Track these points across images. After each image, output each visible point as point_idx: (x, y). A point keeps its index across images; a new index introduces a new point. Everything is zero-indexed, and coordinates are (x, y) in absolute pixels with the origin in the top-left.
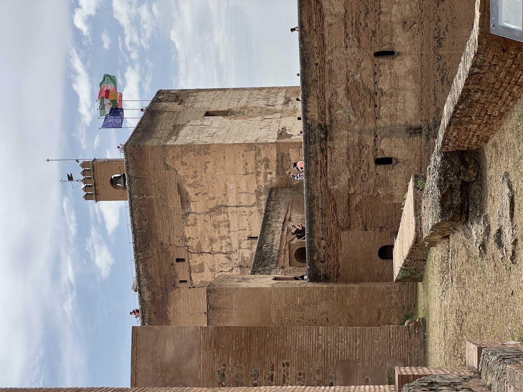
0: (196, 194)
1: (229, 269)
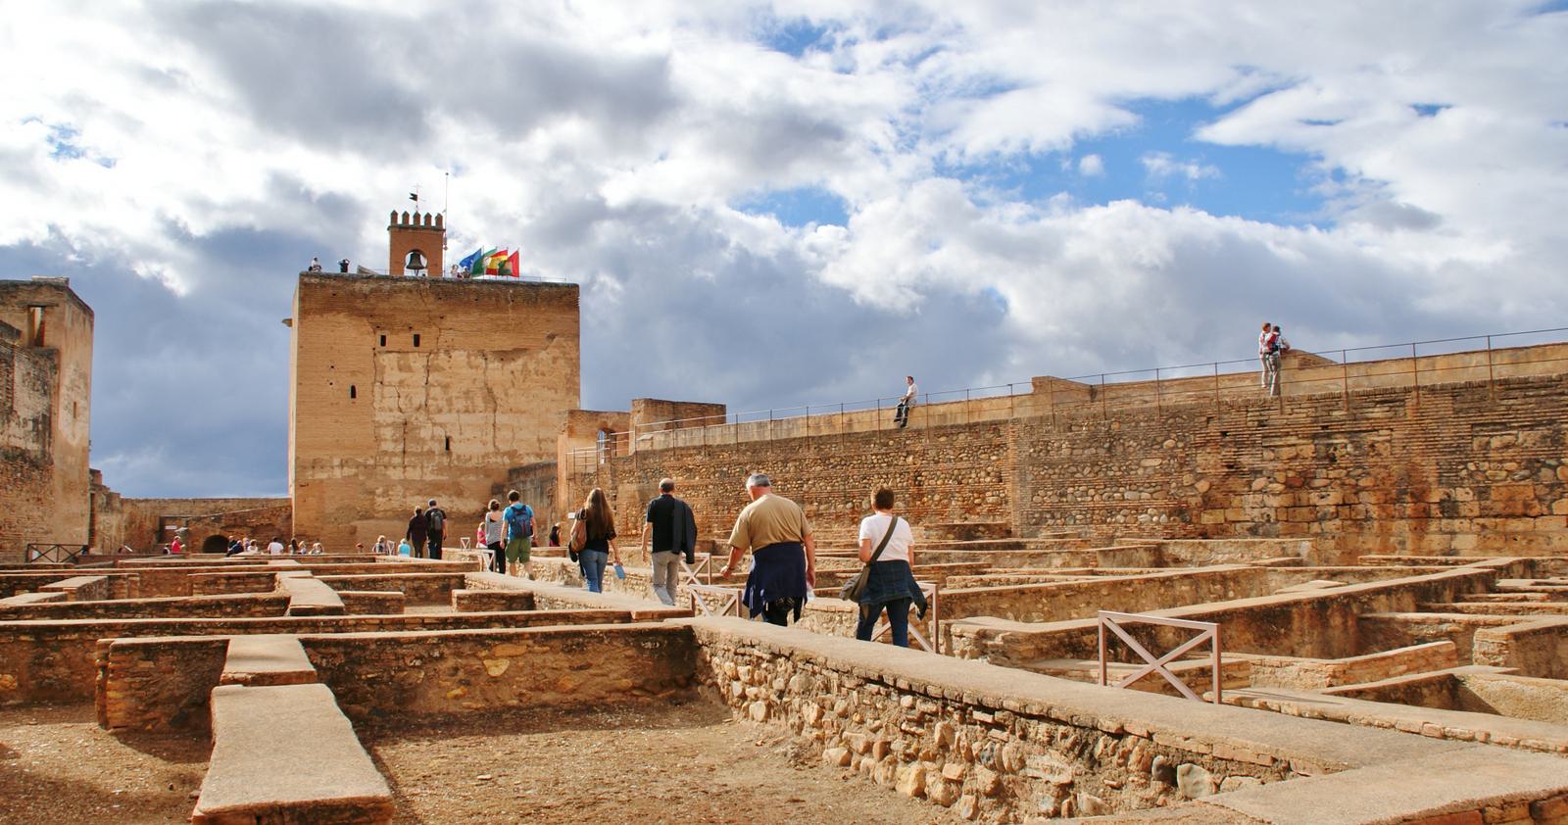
1: (403, 407)
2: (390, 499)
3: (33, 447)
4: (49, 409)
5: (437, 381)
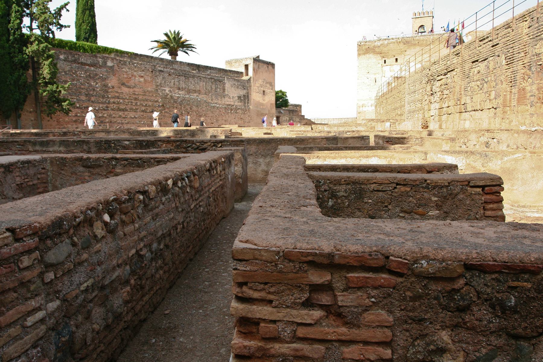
3: (238, 104)
4: (248, 93)
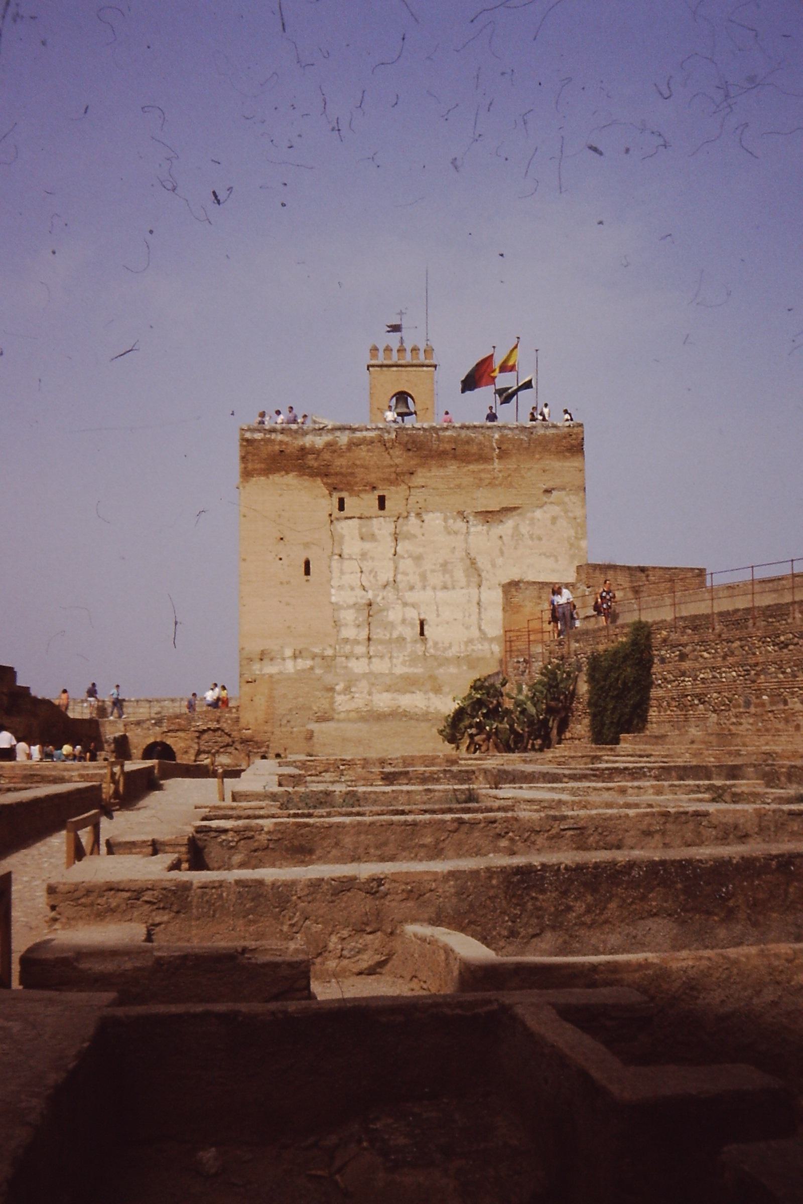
0: (501, 537)
2: (353, 697)
5: (407, 551)
